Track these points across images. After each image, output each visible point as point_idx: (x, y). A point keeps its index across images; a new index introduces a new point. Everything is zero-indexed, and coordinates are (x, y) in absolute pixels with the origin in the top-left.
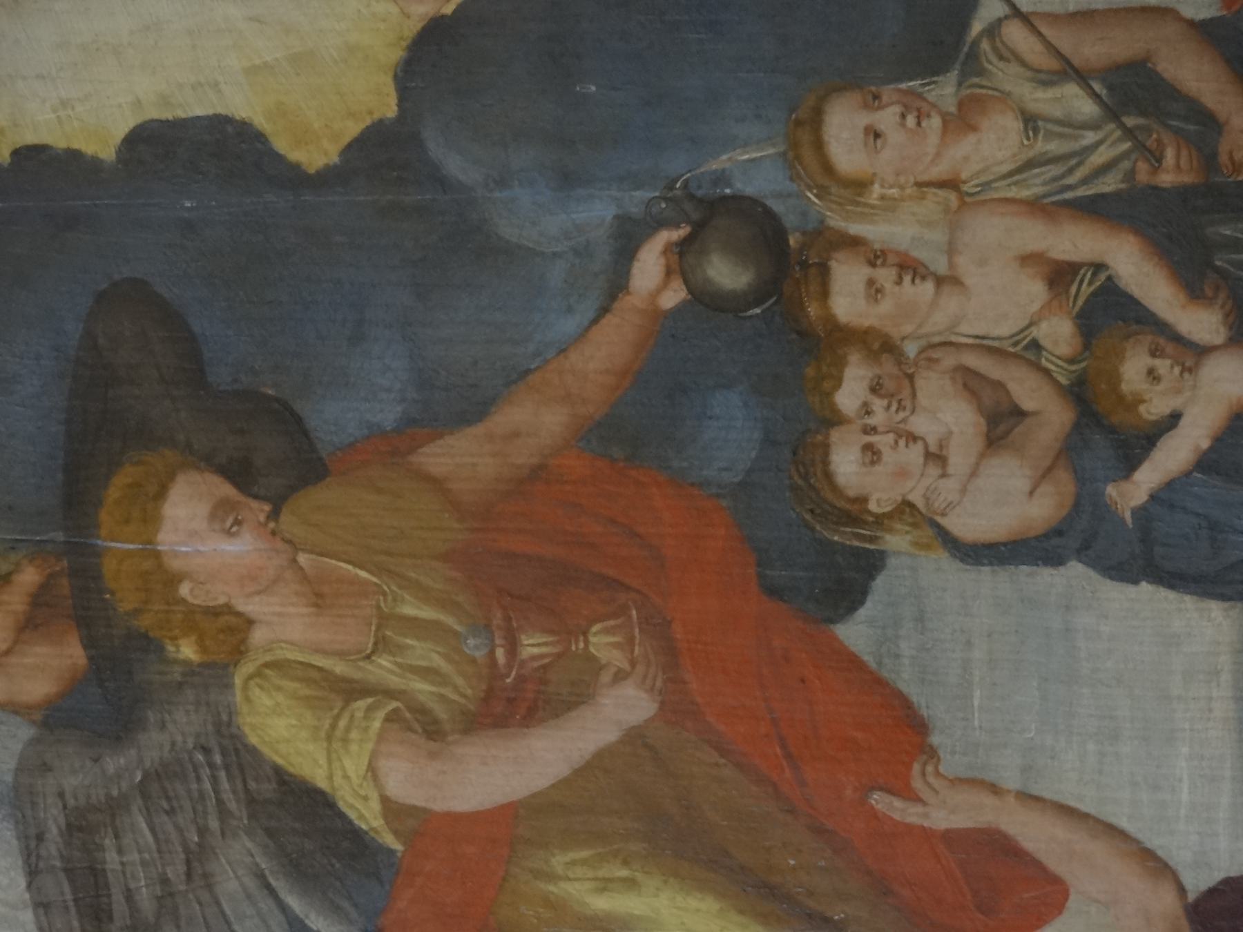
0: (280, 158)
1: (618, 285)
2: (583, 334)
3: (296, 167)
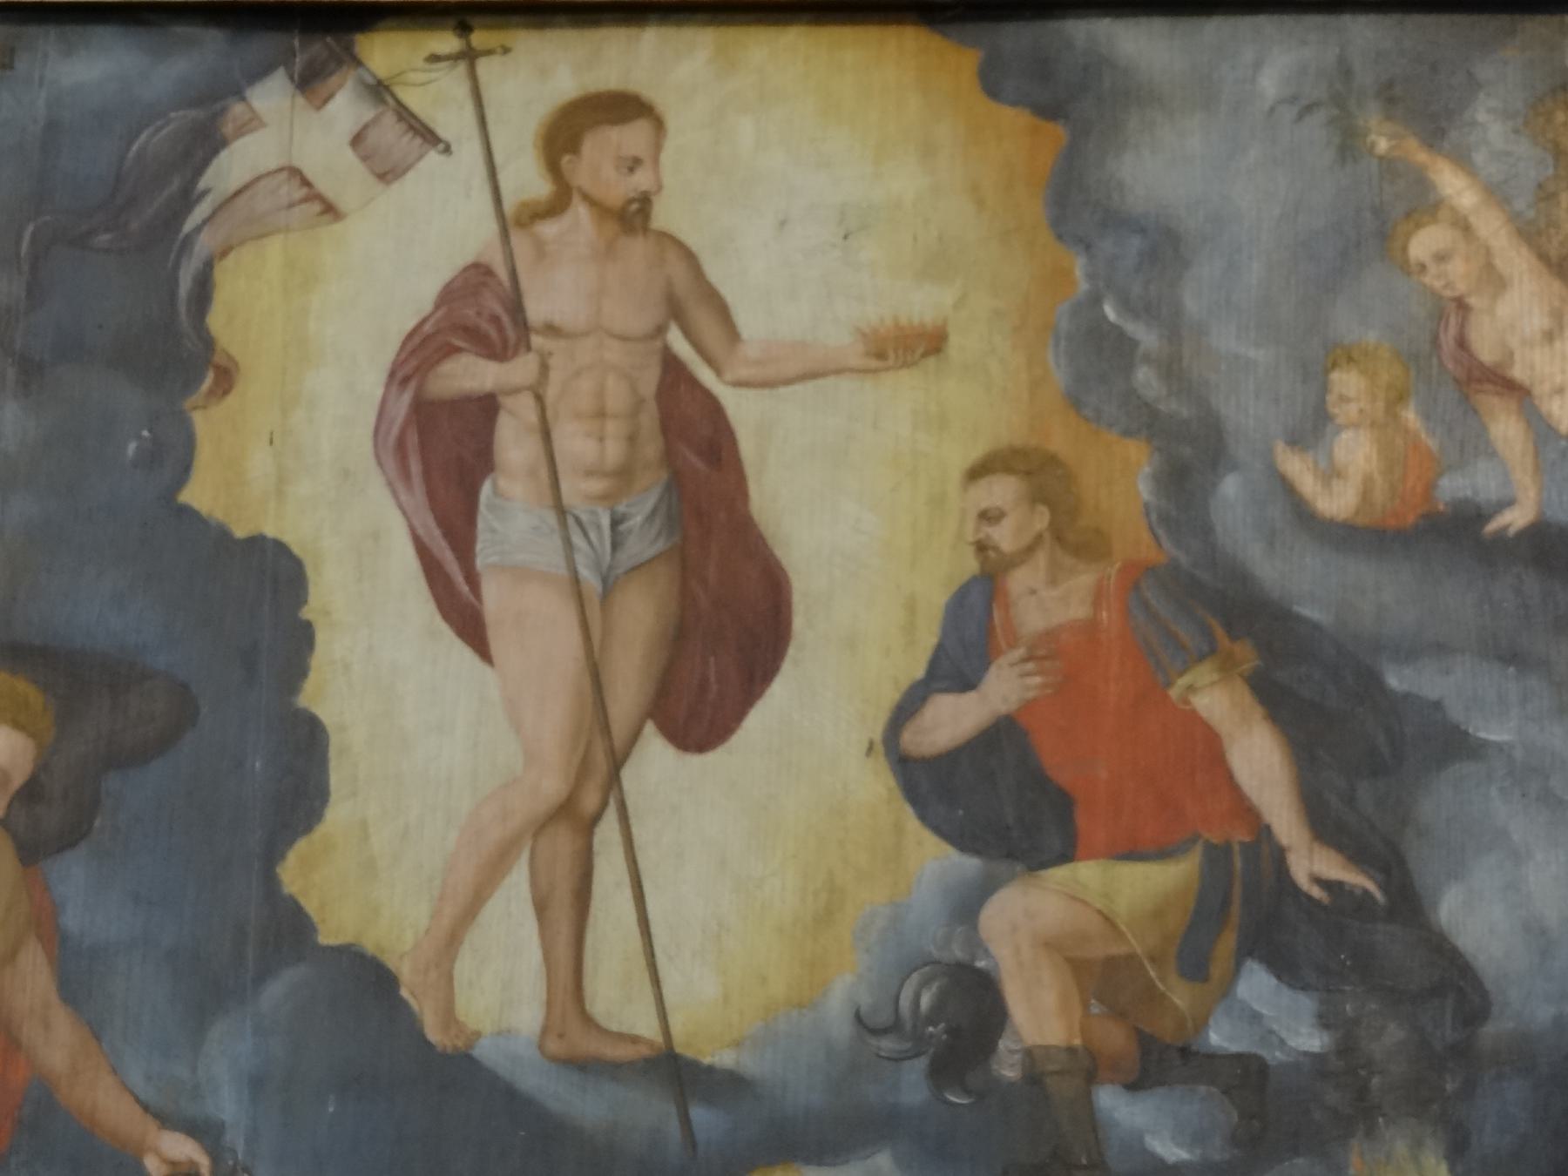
0: (290, 843)
1: (166, 1120)
2: (126, 1087)
3: (283, 856)
